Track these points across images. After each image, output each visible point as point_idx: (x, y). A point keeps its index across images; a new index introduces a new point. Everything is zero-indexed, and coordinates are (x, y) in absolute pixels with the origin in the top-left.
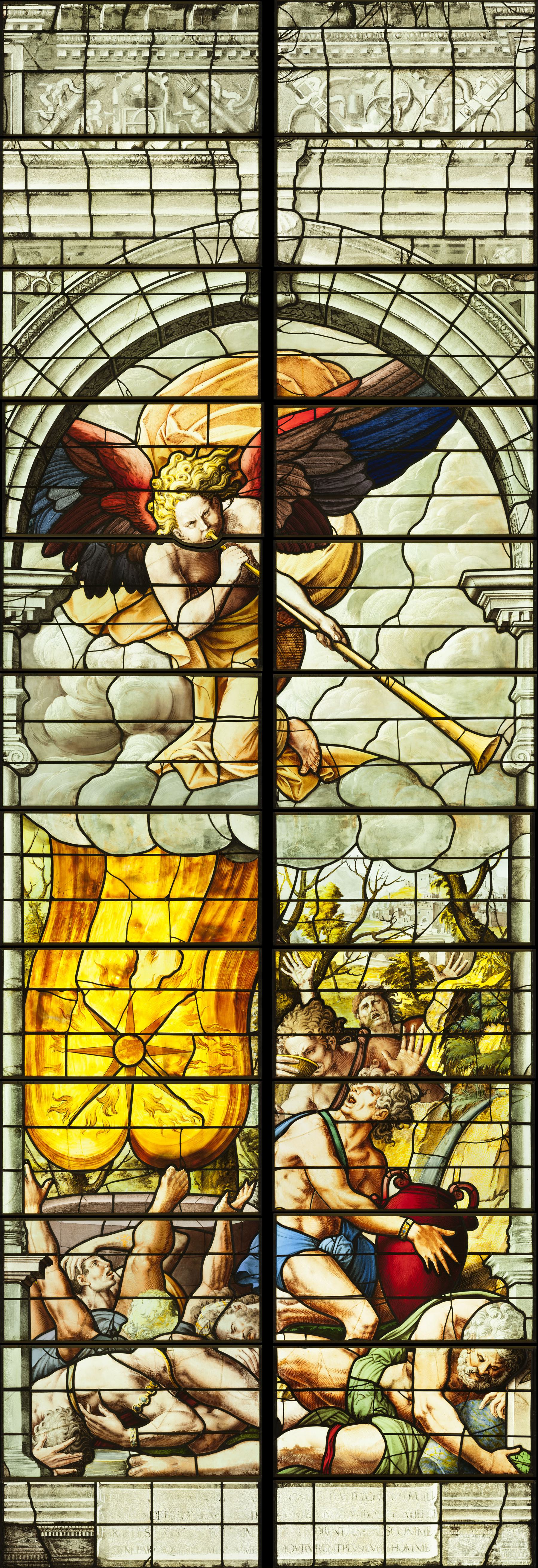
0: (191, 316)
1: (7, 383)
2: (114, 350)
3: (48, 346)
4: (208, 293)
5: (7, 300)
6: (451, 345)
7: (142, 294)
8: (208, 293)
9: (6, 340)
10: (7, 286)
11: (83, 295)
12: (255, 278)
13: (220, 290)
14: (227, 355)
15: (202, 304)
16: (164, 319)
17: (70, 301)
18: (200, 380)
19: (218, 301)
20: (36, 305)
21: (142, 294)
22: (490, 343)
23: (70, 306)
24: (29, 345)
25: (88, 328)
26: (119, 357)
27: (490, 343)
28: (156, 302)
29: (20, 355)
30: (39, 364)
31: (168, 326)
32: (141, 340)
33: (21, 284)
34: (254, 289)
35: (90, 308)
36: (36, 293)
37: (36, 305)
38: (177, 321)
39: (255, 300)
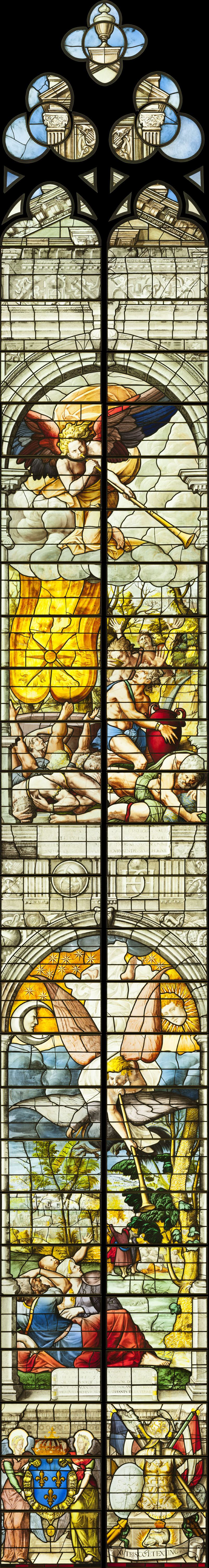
0: (74, 370)
1: (3, 396)
2: (44, 383)
3: (19, 382)
4: (81, 361)
5: (3, 364)
6: (174, 381)
7: (55, 361)
8: (81, 361)
9: (2, 379)
10: (3, 358)
11: (32, 362)
12: (99, 355)
13: (85, 360)
14: (88, 385)
15: (79, 365)
16: (64, 371)
17: (27, 364)
18: (78, 395)
19: (85, 364)
20: (14, 365)
21: (55, 361)
22: (191, 381)
23: (27, 366)
24: (11, 381)
25: (34, 375)
26: (46, 386)
27: (191, 381)
28: (60, 365)
29: (8, 386)
30: (15, 389)
31: (65, 374)
32: (55, 379)
33: (8, 358)
34: (99, 359)
35: (35, 367)
36: (14, 361)
37: (14, 365)
38: (69, 372)
39: (99, 364)
